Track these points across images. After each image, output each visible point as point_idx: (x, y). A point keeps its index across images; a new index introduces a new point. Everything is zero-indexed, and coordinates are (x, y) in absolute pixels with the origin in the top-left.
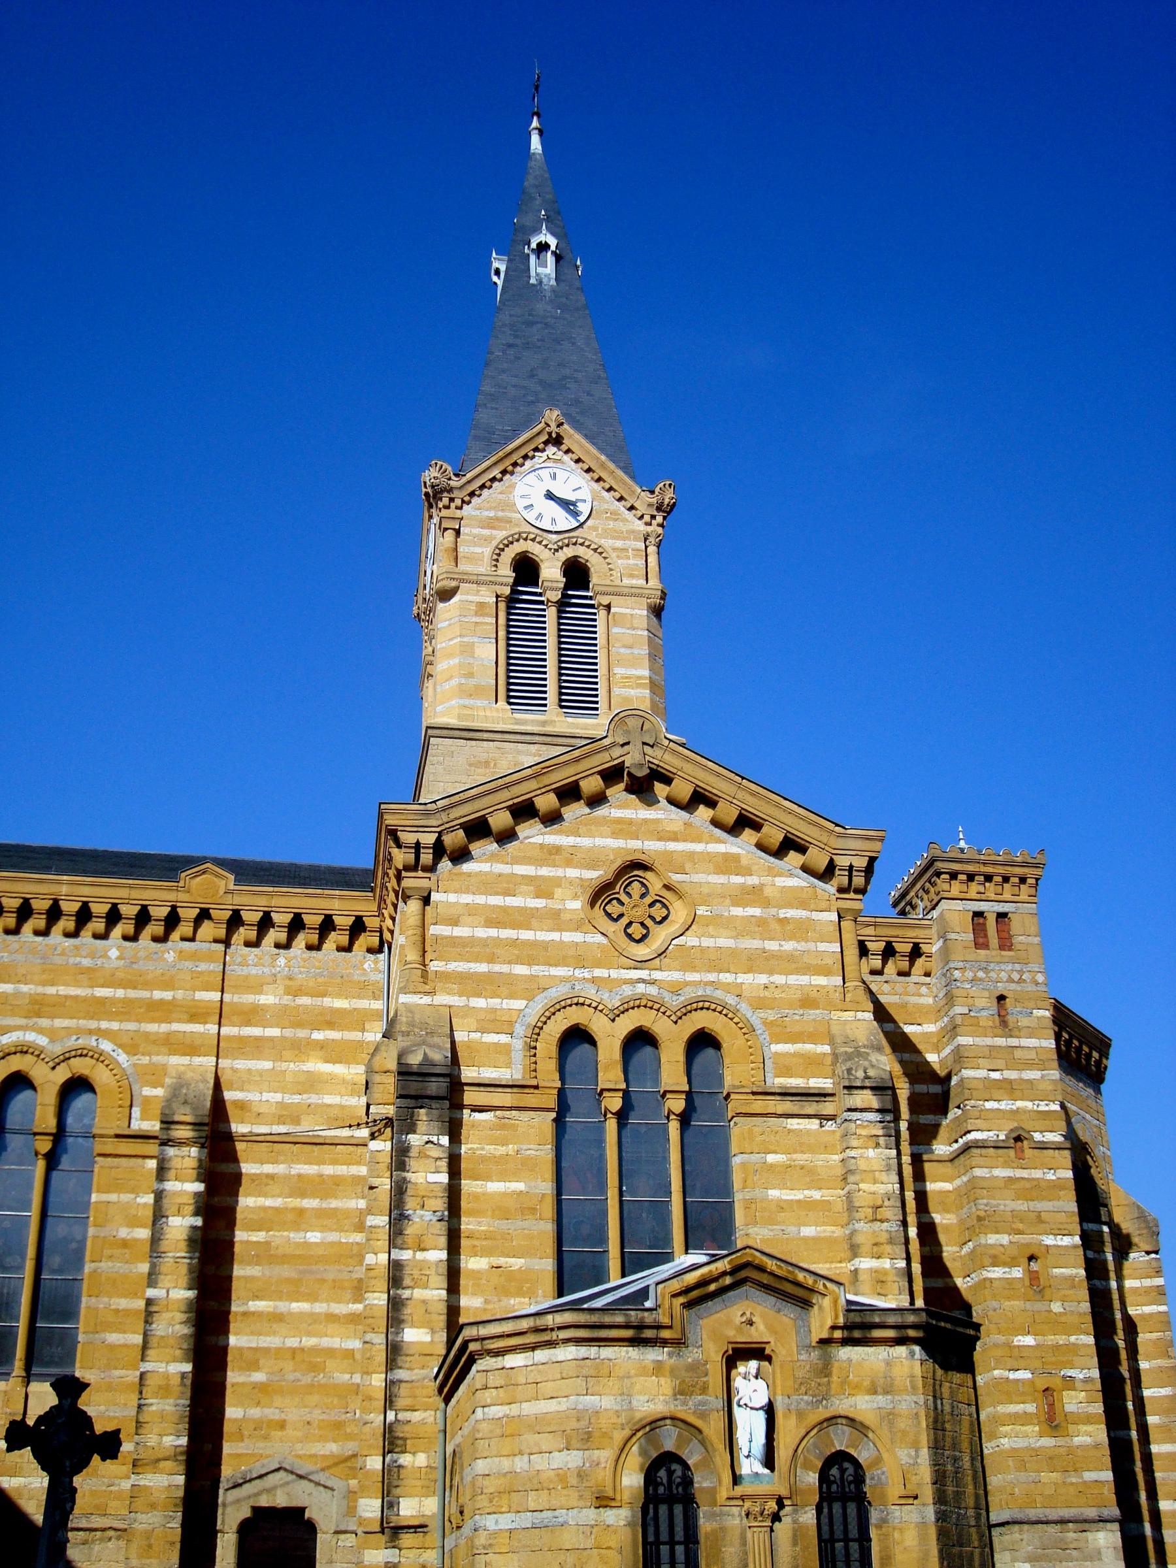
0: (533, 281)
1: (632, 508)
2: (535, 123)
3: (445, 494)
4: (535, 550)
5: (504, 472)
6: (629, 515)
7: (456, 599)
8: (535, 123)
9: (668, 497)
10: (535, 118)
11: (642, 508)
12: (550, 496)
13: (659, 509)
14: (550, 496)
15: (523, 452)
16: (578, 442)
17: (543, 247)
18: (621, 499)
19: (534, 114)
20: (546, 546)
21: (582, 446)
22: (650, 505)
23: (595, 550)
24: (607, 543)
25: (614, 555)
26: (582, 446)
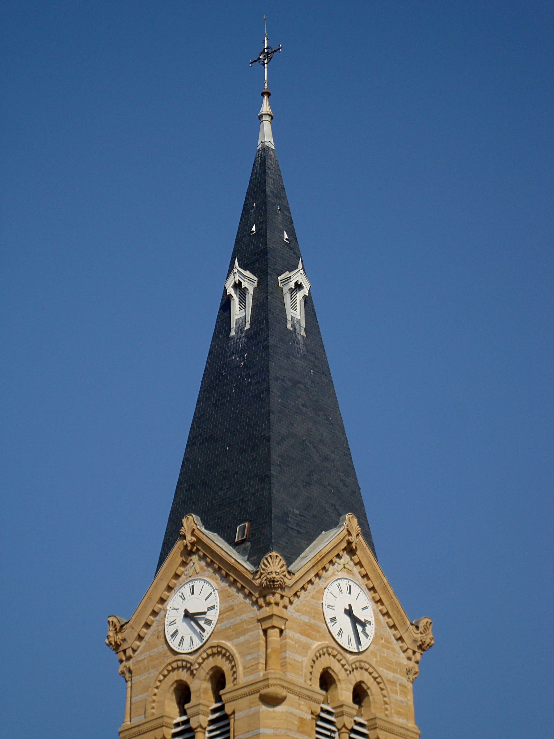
0: (289, 326)
1: (400, 639)
2: (266, 108)
3: (279, 591)
4: (336, 667)
5: (317, 575)
6: (397, 645)
7: (279, 709)
8: (266, 108)
9: (428, 638)
10: (266, 98)
11: (408, 642)
12: (349, 612)
13: (420, 647)
14: (349, 612)
15: (329, 558)
16: (368, 558)
17: (299, 286)
18: (394, 627)
19: (263, 94)
20: (343, 666)
21: (371, 563)
22: (415, 641)
23: (375, 678)
24: (383, 671)
25: (389, 687)
26: (371, 563)
